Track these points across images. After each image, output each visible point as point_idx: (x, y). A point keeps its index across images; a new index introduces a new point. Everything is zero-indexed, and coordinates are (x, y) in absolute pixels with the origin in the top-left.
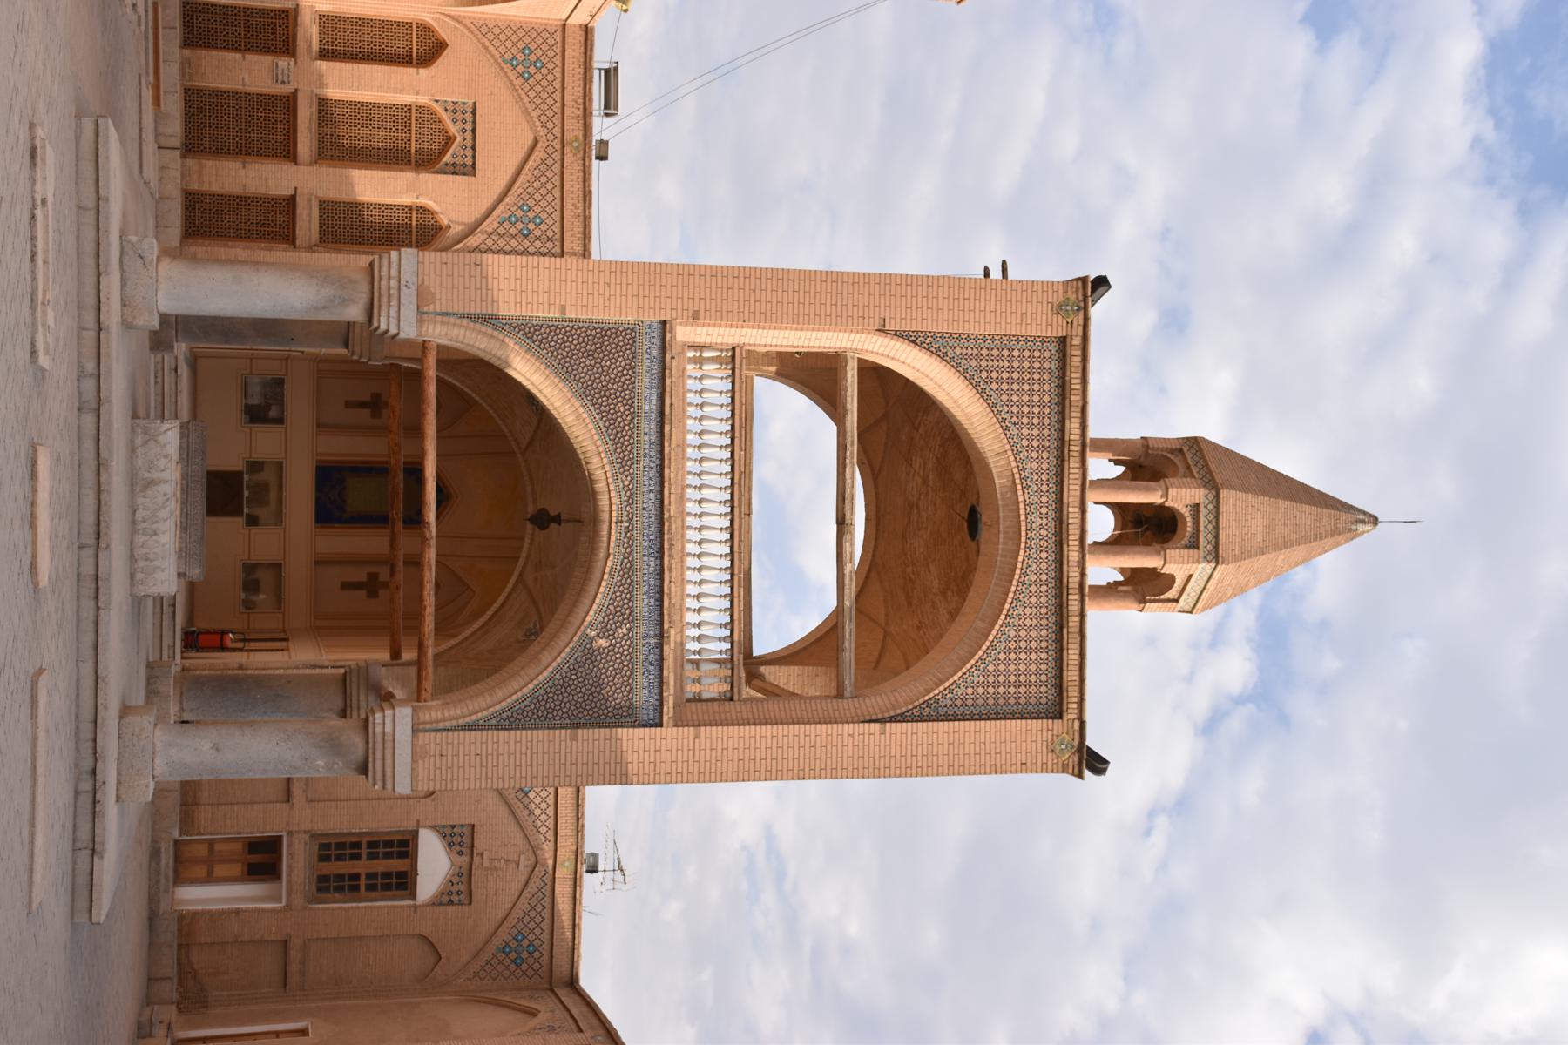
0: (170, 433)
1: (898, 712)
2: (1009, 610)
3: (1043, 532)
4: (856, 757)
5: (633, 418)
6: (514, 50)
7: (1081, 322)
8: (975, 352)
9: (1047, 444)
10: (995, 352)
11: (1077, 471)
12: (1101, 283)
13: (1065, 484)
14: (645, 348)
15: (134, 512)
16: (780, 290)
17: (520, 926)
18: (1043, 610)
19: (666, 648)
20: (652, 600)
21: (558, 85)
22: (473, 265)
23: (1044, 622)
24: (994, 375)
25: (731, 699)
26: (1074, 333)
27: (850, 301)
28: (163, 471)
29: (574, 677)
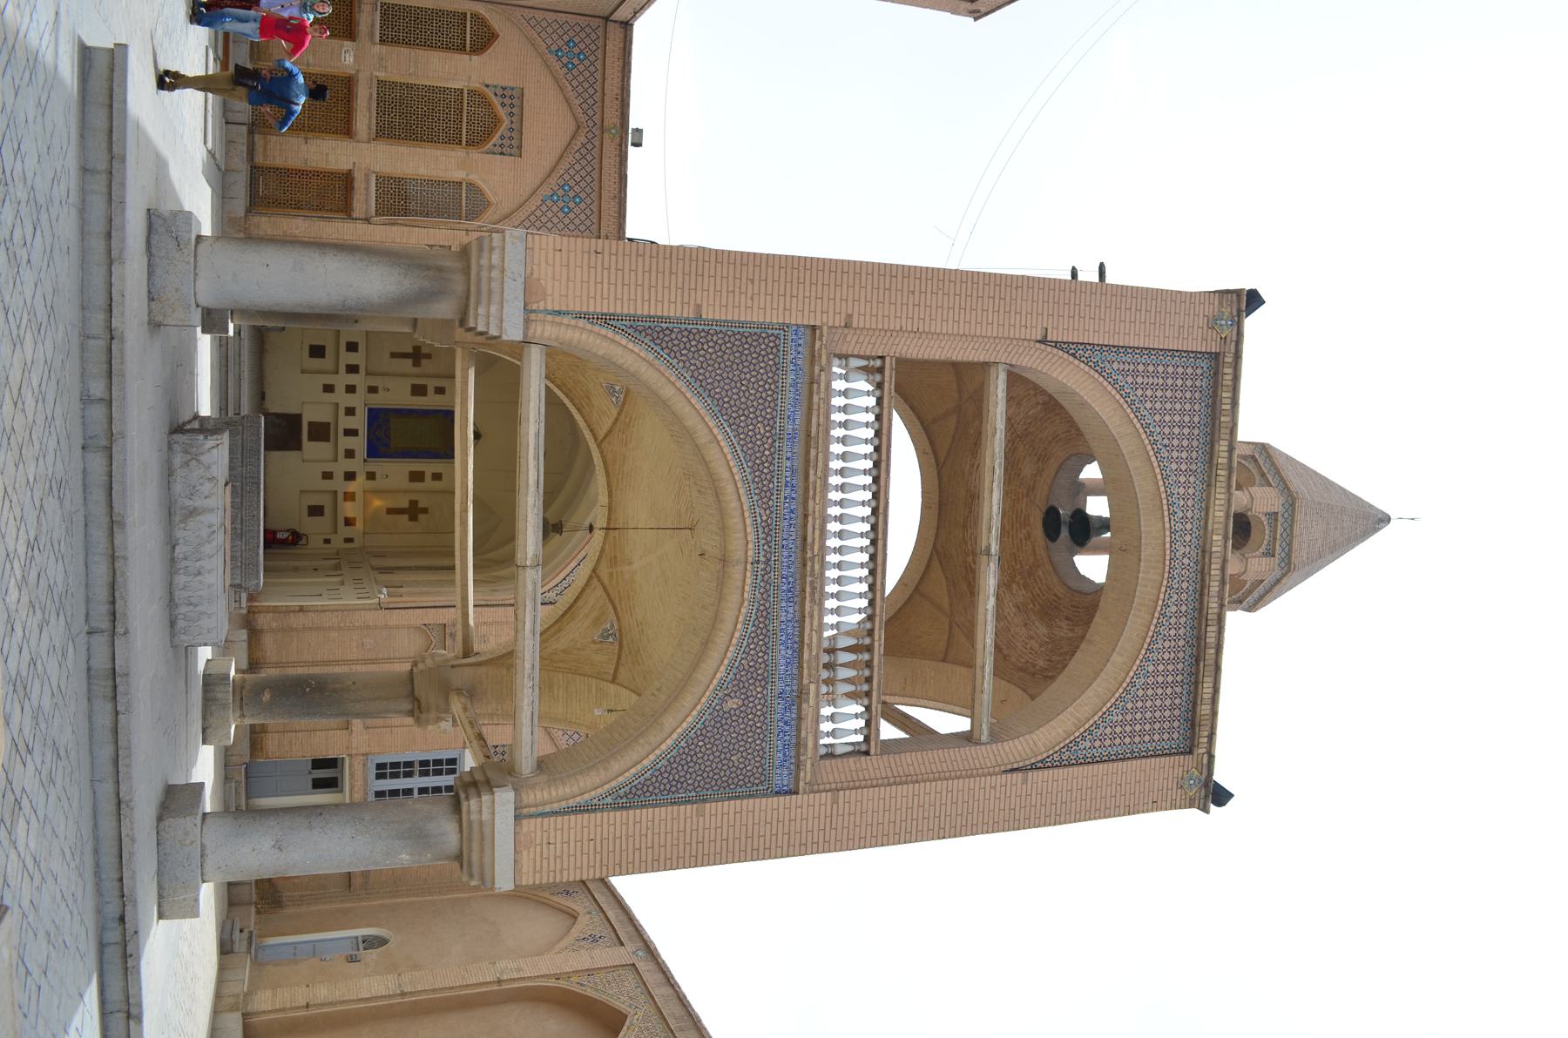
0: (215, 451)
1: (1039, 758)
4: (997, 810)
5: (775, 441)
6: (560, 43)
7: (1234, 338)
8: (1132, 367)
9: (1194, 467)
10: (1151, 368)
11: (1222, 496)
12: (1253, 300)
13: (1211, 510)
14: (790, 357)
15: (173, 547)
16: (940, 292)
18: (1181, 643)
20: (790, 652)
21: (598, 76)
22: (593, 253)
23: (1181, 655)
24: (1149, 393)
27: (1013, 308)
28: (206, 497)
29: (700, 744)
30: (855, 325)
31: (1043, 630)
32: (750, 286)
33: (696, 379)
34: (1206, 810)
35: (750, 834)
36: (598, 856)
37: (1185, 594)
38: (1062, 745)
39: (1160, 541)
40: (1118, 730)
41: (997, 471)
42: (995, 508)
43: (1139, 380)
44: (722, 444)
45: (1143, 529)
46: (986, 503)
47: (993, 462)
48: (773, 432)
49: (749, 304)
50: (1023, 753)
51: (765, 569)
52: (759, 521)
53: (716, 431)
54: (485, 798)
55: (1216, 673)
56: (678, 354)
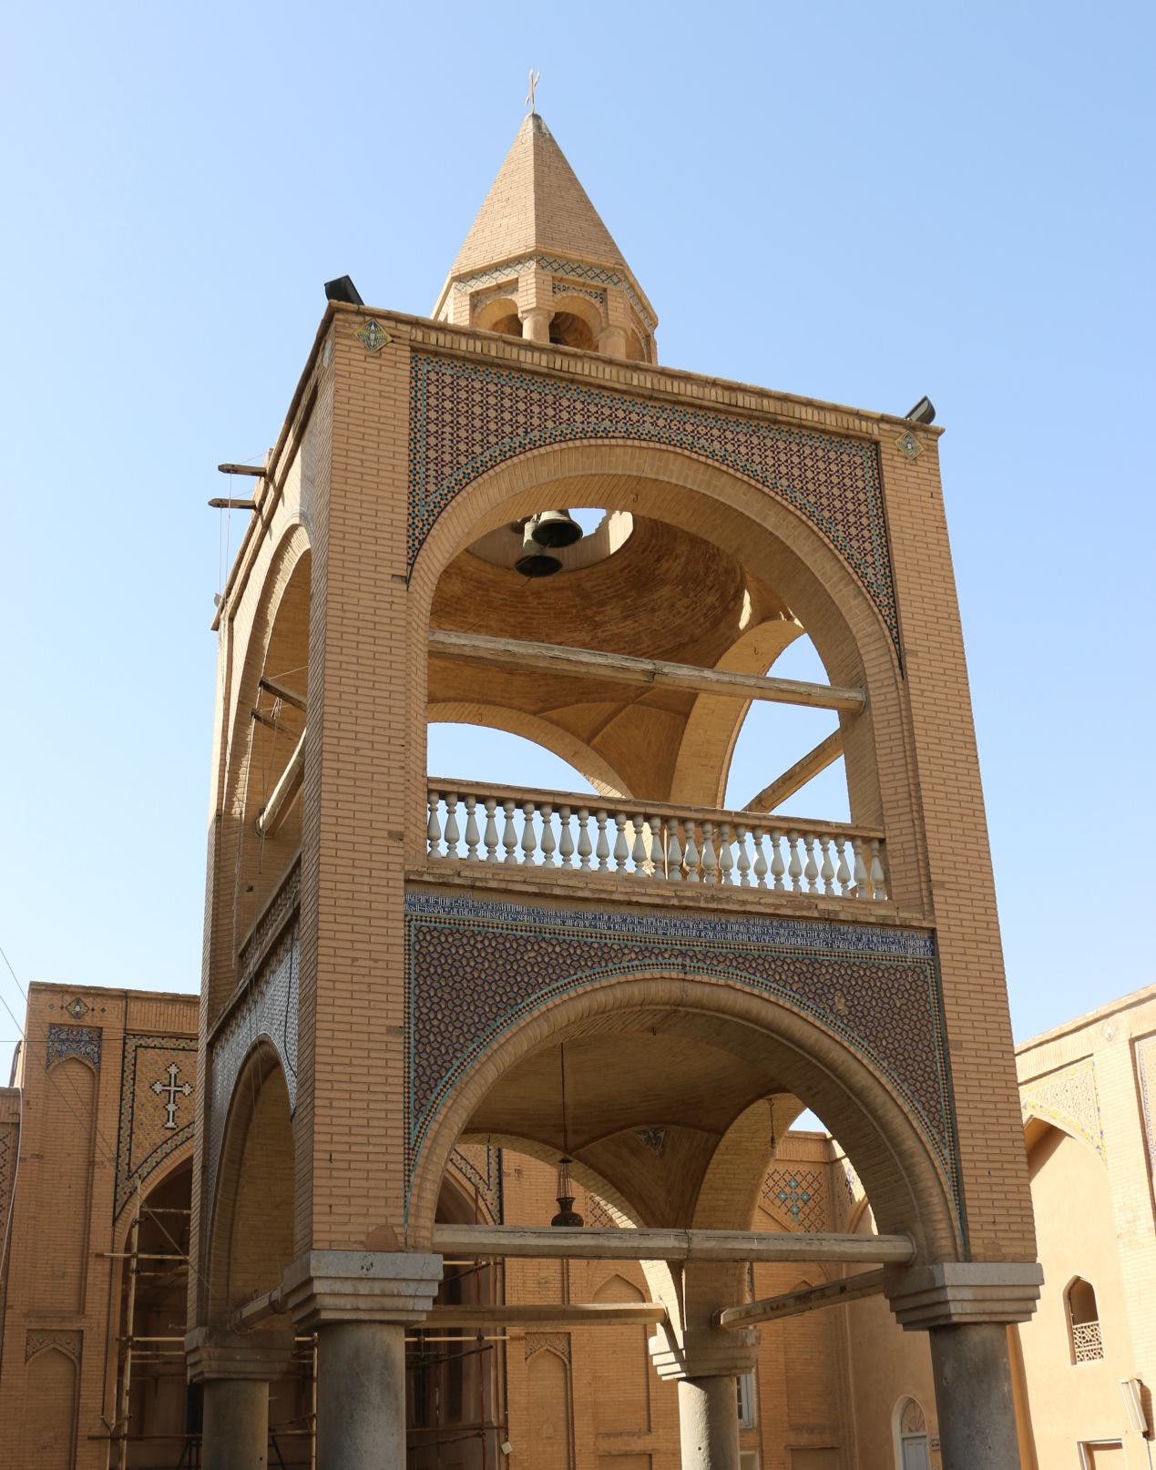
1: (887, 633)
2: (757, 481)
3: (661, 422)
5: (544, 939)
7: (392, 324)
8: (431, 466)
9: (550, 399)
11: (586, 366)
13: (603, 383)
16: (355, 713)
17: (772, 1195)
19: (842, 917)
20: (782, 931)
22: (332, 1165)
24: (463, 447)
25: (882, 841)
26: (407, 336)
27: (369, 618)
30: (400, 828)
31: (665, 591)
32: (360, 963)
33: (475, 1035)
34: (939, 432)
35: (979, 988)
36: (1006, 1166)
37: (699, 429)
38: (872, 603)
39: (637, 451)
40: (853, 531)
41: (556, 653)
42: (601, 660)
43: (447, 458)
44: (550, 1005)
45: (620, 472)
46: (593, 670)
47: (544, 657)
48: (533, 940)
49: (382, 964)
50: (880, 652)
51: (691, 958)
52: (636, 962)
53: (536, 1013)
54: (950, 1294)
55: (791, 401)
56: (447, 1058)
